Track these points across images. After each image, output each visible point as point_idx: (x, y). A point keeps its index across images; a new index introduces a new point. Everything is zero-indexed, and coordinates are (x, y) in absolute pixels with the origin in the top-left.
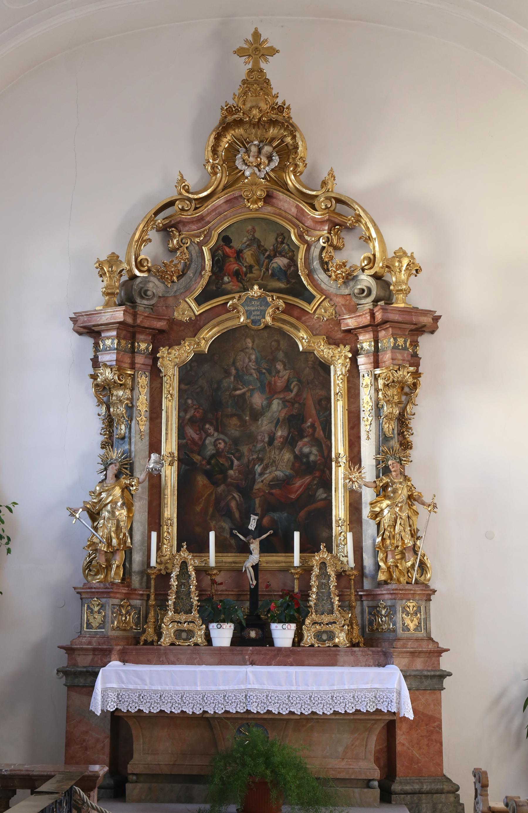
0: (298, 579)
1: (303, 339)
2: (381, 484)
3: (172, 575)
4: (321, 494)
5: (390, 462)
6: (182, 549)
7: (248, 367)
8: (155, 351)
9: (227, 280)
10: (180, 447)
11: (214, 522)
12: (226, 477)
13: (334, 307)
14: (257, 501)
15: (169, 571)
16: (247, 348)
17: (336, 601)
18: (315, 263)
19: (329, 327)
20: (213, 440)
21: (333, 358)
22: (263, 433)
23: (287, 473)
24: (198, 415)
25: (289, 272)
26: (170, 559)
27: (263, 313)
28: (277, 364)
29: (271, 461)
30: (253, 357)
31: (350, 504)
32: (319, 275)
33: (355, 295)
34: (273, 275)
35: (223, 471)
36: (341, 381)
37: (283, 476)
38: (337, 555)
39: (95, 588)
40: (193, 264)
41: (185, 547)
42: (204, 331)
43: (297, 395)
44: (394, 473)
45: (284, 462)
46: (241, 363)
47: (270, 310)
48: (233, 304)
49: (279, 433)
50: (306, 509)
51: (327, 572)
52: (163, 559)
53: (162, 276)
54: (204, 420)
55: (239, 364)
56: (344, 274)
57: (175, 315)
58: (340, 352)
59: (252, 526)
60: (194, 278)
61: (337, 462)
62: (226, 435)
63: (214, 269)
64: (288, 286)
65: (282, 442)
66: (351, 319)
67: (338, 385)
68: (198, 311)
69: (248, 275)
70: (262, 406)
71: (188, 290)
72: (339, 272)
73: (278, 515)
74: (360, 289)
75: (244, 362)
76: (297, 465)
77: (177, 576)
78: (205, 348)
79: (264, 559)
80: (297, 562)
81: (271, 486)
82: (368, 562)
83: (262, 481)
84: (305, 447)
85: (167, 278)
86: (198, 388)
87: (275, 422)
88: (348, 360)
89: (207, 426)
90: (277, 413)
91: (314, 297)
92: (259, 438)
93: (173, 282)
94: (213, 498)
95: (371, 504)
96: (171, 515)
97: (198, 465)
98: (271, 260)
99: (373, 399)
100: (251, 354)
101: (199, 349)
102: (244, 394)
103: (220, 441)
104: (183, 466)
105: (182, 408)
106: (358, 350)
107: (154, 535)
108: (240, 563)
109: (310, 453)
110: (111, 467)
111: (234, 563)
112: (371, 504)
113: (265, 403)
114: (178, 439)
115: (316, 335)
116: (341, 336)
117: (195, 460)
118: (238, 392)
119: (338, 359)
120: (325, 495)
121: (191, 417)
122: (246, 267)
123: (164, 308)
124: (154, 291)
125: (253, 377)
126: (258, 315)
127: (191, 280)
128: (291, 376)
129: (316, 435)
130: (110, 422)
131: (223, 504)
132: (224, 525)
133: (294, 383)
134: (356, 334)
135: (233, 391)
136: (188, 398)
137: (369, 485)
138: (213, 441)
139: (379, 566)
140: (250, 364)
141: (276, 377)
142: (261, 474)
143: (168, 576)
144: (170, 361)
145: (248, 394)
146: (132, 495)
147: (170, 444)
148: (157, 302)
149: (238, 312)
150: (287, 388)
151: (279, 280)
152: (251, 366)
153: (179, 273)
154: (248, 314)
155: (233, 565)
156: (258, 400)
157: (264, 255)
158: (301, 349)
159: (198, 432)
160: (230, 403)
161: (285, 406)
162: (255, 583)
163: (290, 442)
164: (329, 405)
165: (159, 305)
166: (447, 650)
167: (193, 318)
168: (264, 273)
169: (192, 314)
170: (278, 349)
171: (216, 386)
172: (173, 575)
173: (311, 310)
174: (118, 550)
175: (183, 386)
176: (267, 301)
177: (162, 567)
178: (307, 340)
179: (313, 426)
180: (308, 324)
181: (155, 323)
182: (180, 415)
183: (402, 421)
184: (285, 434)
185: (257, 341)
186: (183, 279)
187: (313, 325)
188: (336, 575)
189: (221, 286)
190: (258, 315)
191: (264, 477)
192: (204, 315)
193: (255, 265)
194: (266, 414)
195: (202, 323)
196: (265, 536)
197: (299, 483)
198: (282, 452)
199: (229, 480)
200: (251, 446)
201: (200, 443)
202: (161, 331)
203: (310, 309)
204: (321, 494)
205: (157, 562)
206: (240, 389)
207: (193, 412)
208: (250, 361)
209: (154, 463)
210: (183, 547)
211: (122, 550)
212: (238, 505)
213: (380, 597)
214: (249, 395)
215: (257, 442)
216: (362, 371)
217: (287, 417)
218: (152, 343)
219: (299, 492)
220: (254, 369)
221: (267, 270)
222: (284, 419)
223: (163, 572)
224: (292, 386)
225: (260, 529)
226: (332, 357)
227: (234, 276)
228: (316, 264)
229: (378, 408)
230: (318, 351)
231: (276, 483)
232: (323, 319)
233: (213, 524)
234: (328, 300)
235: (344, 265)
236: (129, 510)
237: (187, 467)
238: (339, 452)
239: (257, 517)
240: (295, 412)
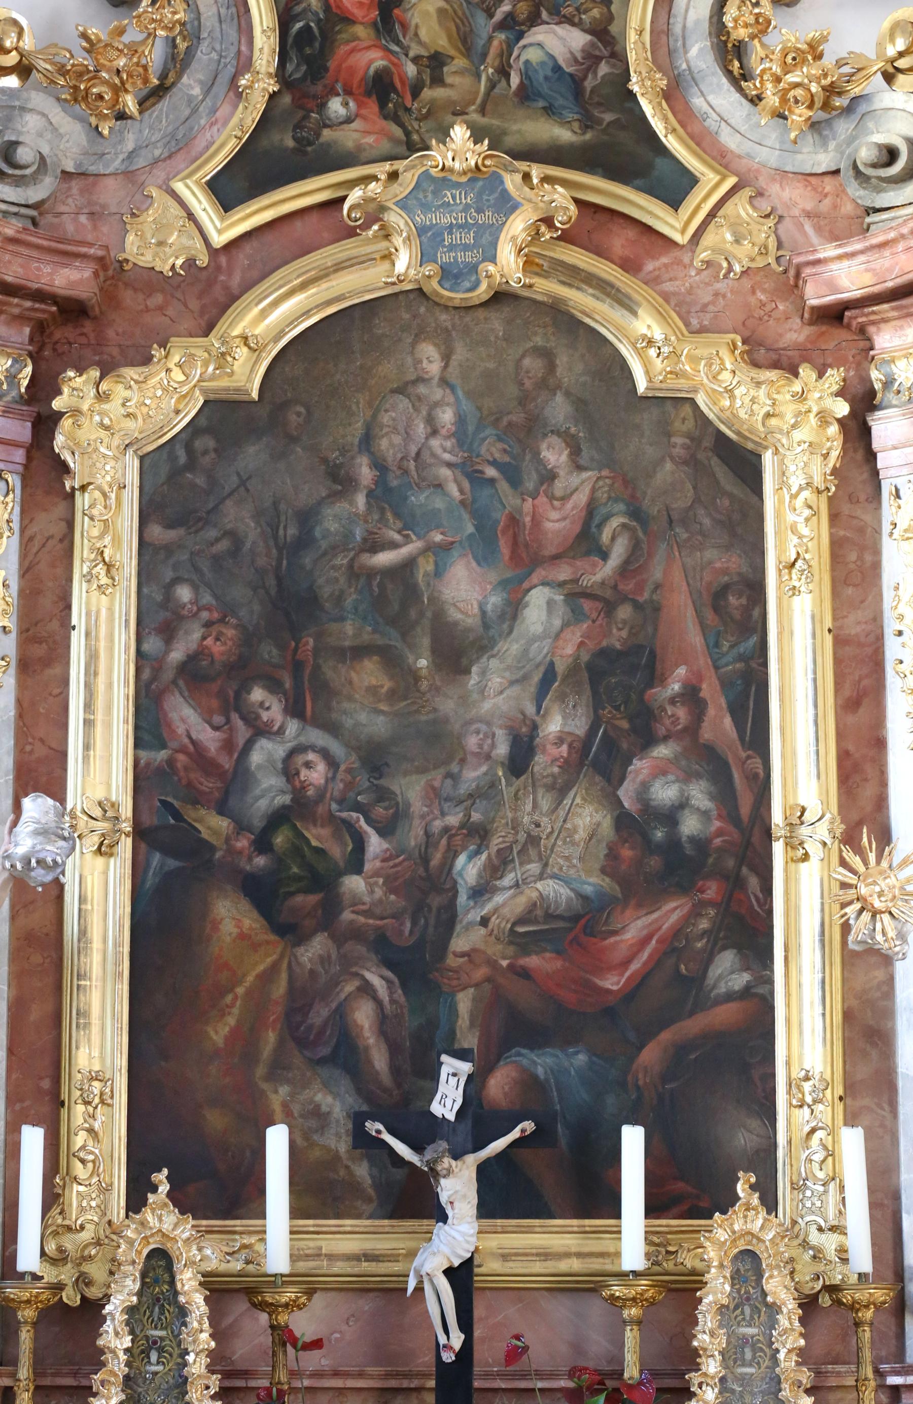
0: (639, 1322)
1: (646, 342)
3: (108, 1308)
4: (727, 972)
6: (151, 1198)
7: (426, 455)
8: (43, 387)
9: (342, 111)
10: (143, 780)
11: (284, 1090)
12: (332, 905)
13: (771, 222)
14: (464, 1002)
15: (94, 1293)
16: (420, 380)
18: (694, 52)
19: (752, 300)
20: (280, 751)
21: (773, 422)
22: (488, 724)
23: (588, 890)
24: (217, 649)
25: (589, 84)
26: (98, 1243)
27: (486, 239)
28: (544, 446)
29: (522, 837)
30: (447, 416)
31: (848, 1016)
32: (710, 98)
33: (858, 173)
34: (526, 94)
35: (322, 879)
37: (569, 899)
38: (794, 1222)
40: (204, 47)
41: (164, 1188)
42: (248, 308)
43: (624, 570)
45: (573, 843)
46: (397, 440)
47: (518, 226)
48: (367, 200)
49: (554, 725)
50: (666, 1036)
51: (764, 1294)
52: (69, 1242)
53: (76, 88)
54: (242, 670)
55: (389, 445)
56: (814, 88)
57: (128, 245)
58: (801, 397)
59: (447, 1102)
60: (209, 102)
61: (793, 843)
62: (333, 729)
63: (290, 67)
64: (588, 136)
65: (566, 761)
66: (846, 263)
67: (794, 529)
68: (220, 232)
69: (427, 94)
70: (483, 613)
71: (180, 148)
72: (792, 78)
73: (549, 1060)
74: (880, 146)
75: (408, 436)
76: (627, 853)
77: (131, 1310)
78: (250, 379)
79: (494, 1242)
80: (633, 1252)
81: (521, 942)
83: (484, 922)
84: (659, 780)
85: (100, 97)
86: (217, 540)
87: (537, 677)
89: (257, 694)
90: (547, 644)
91: (692, 181)
92: (472, 742)
93: (121, 116)
94: (280, 989)
96: (102, 1058)
97: (218, 855)
98: (520, 36)
100: (437, 404)
101: (224, 383)
102: (409, 564)
103: (311, 756)
104: (157, 858)
105: (156, 619)
106: (872, 393)
107: (33, 1139)
108: (391, 1257)
109: (683, 805)
111: (369, 1257)
113: (495, 600)
114: (136, 746)
115: (702, 330)
116: (801, 338)
117: (205, 834)
118: (384, 558)
119: (794, 427)
120: (746, 977)
121: (192, 659)
122: (416, 60)
123: (83, 219)
124: (46, 151)
125: (446, 494)
126: (466, 248)
127: (194, 111)
128: (602, 495)
129: (707, 734)
131: (320, 1014)
132: (324, 1100)
133: (615, 522)
134: (862, 330)
135: (363, 550)
136: (176, 581)
138: (280, 757)
140: (435, 443)
141: (542, 499)
142: (480, 892)
143: (92, 1311)
144: (107, 428)
145: (426, 566)
147: (102, 767)
148: (53, 196)
149: (387, 237)
150: (586, 541)
151: (550, 111)
152: (439, 451)
153: (146, 81)
154: (428, 241)
155: (366, 1267)
156: (465, 589)
157: (491, 16)
158: (642, 386)
159: (218, 719)
160: (349, 602)
161: (576, 615)
162: (457, 1340)
163: (600, 760)
164: (756, 613)
165: (63, 208)
167: (203, 260)
168: (492, 85)
169: (199, 244)
170: (547, 384)
171: (292, 531)
172: (115, 1308)
173: (683, 232)
175: (156, 531)
176: (505, 191)
177: (67, 1274)
178: (666, 350)
179: (691, 695)
180: (668, 287)
181: (47, 269)
182: (146, 647)
184: (579, 726)
185: (461, 353)
186: (164, 104)
187: (690, 292)
188: (800, 1306)
189: (318, 135)
190: (466, 248)
191: (490, 909)
192: (248, 248)
193: (452, 52)
194: (502, 646)
195: (236, 281)
196: (499, 1145)
197: (637, 931)
198: (567, 802)
199: (347, 916)
200: (436, 777)
201: (227, 763)
202: (72, 310)
203: (678, 226)
204: (727, 972)
205: (43, 1253)
206: (394, 546)
207: (197, 635)
208: (434, 432)
209: (37, 833)
210: (154, 1189)
212: (383, 1021)
214: (430, 568)
215: (463, 761)
216: (892, 472)
217: (585, 657)
218: (30, 355)
219: (635, 966)
220: (449, 465)
221: (504, 72)
222: (574, 669)
223: (71, 1297)
224: (606, 536)
225: (478, 1120)
226: (768, 415)
227: (368, 94)
228: (698, 54)
230: (713, 396)
231: (547, 929)
232: (730, 269)
233: (278, 1096)
234: (747, 192)
235: (815, 50)
237: (172, 864)
238: (802, 802)
239: (466, 1068)
240: (617, 638)
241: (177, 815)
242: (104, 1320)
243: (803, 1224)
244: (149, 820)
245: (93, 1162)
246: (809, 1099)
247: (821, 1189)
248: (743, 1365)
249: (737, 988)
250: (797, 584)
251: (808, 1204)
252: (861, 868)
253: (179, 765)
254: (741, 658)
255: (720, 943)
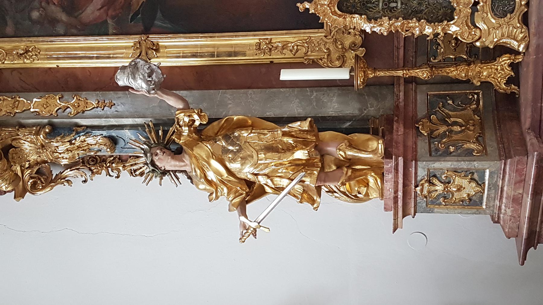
10: (122, 31)
15: (359, 40)
39: (396, 192)
52: (335, 56)
104: (157, 22)
105: (49, 28)
107: (286, 75)
110: (157, 163)
114: (107, 34)
130: (93, 163)
143: (368, 39)
146: (211, 121)
174: (316, 147)
175: (9, 30)
177: (351, 55)
182: (62, 32)
205: (340, 67)
207: (53, 7)
209: (134, 78)
211: (317, 136)
236: (242, 125)
237: (159, 15)
241: (136, 14)
242: (374, 32)
244: (141, 28)
245: (297, 46)
253: (114, 14)
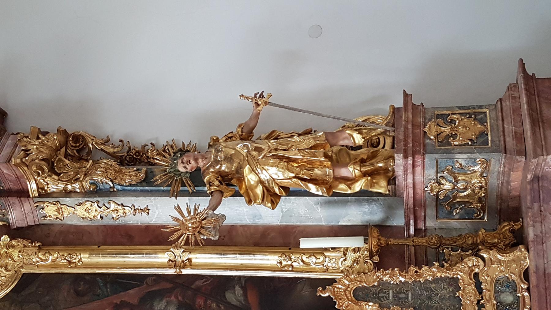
2: (217, 183)
4: (235, 296)
5: (181, 168)
17: (430, 273)
21: (9, 267)
36: (47, 254)
38: (342, 272)
44: (201, 163)
82: (355, 215)
88: (14, 242)
95: (250, 202)
99: (81, 200)
112: (250, 202)
119: (12, 259)
120: (237, 288)
129: (135, 301)
137: (214, 203)
139: (362, 193)
164: (87, 278)
166: (522, 64)
183: (132, 158)
188: (379, 270)
213: (419, 191)
229: (96, 192)
238: (167, 260)
243: (343, 268)
246: (290, 263)
247: (327, 259)
248: (408, 298)
249: (242, 292)
250: (77, 260)
251: (334, 265)
252: (179, 233)
254: (105, 285)
255: (223, 299)
